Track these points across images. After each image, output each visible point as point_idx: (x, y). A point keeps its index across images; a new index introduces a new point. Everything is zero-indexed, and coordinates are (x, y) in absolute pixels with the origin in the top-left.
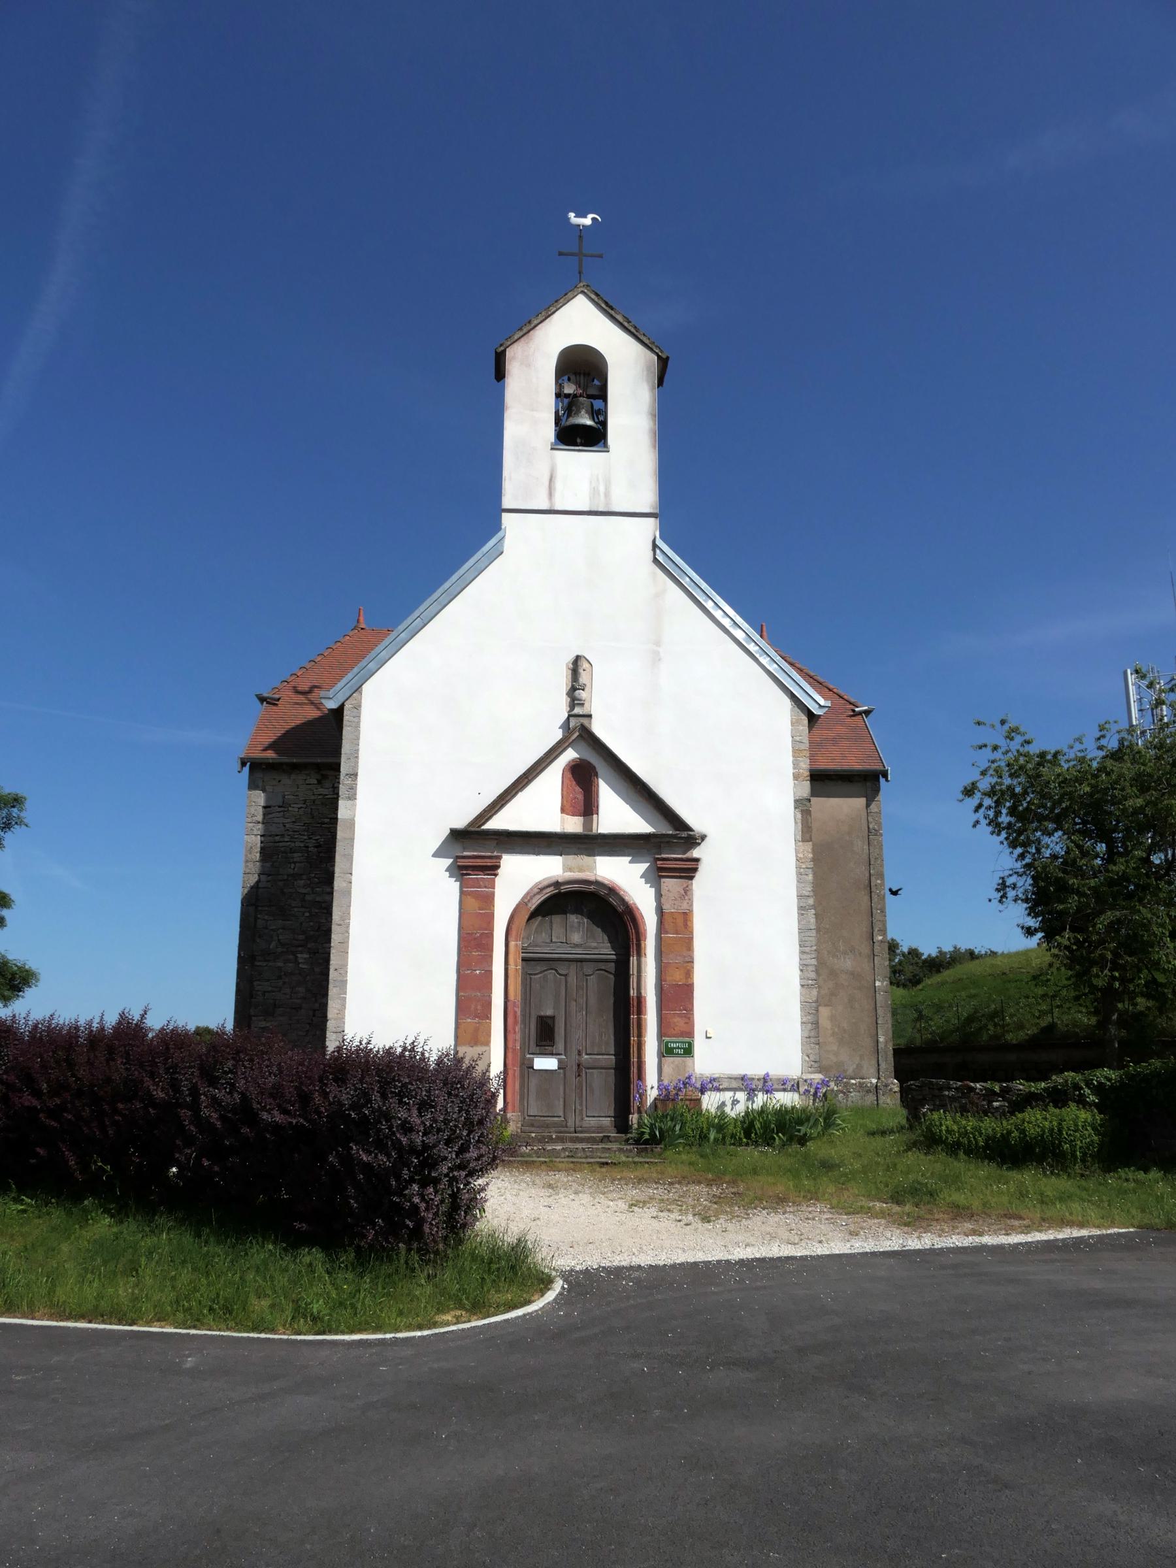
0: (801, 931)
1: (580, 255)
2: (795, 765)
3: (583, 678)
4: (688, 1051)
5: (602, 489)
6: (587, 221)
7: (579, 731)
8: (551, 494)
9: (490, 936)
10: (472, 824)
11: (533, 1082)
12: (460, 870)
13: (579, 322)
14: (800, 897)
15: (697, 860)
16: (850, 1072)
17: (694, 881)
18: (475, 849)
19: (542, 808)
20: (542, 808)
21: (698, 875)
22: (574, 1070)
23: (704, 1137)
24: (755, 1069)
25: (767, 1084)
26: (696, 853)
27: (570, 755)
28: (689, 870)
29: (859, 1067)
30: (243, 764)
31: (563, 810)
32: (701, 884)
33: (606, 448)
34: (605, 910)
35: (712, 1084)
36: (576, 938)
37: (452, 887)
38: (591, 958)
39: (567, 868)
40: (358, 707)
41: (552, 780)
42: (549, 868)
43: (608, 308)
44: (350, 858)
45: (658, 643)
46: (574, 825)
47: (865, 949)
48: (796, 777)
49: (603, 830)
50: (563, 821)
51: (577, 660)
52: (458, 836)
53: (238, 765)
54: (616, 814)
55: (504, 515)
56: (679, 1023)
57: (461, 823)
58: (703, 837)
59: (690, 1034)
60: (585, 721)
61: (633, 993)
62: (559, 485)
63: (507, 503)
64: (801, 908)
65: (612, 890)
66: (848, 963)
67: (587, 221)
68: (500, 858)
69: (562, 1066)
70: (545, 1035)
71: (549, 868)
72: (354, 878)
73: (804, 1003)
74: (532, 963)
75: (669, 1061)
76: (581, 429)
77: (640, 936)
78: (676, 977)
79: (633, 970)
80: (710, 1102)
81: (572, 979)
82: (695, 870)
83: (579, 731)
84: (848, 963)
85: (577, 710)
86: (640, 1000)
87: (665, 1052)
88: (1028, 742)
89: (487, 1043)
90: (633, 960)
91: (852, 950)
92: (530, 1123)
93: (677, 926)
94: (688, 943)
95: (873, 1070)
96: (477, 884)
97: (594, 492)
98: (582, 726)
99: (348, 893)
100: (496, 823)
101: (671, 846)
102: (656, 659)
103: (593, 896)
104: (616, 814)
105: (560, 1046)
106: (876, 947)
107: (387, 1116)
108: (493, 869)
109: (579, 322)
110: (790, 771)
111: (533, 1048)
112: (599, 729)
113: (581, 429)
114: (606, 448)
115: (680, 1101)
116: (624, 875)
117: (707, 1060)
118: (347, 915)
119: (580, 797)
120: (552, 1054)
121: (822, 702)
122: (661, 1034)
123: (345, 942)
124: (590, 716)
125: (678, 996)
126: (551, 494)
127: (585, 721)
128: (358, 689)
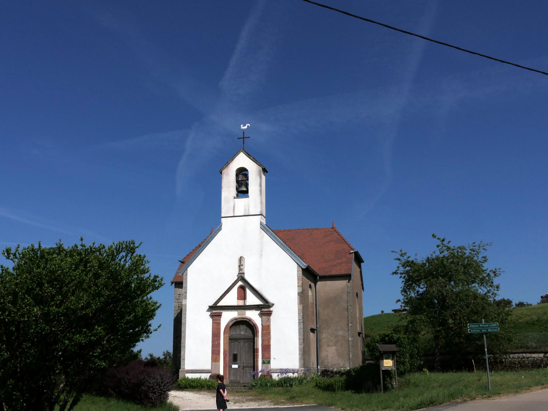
0: (299, 329)
1: (244, 138)
2: (298, 283)
3: (242, 263)
4: (269, 362)
5: (247, 209)
6: (246, 127)
7: (241, 277)
8: (234, 212)
9: (219, 333)
10: (214, 304)
11: (232, 371)
12: (212, 316)
13: (242, 160)
14: (299, 320)
15: (272, 311)
16: (341, 366)
17: (271, 317)
18: (216, 310)
19: (232, 299)
20: (232, 299)
21: (272, 315)
22: (243, 367)
23: (267, 385)
24: (285, 367)
25: (287, 371)
26: (271, 309)
27: (240, 283)
28: (269, 314)
29: (344, 364)
30: (172, 283)
31: (238, 299)
32: (272, 317)
33: (248, 197)
34: (249, 324)
35: (275, 371)
36: (242, 333)
37: (210, 321)
38: (243, 339)
39: (239, 315)
40: (187, 274)
41: (234, 292)
42: (234, 315)
43: (249, 155)
44: (185, 314)
45: (262, 251)
46: (241, 303)
47: (346, 329)
48: (298, 286)
49: (247, 304)
50: (238, 302)
51: (241, 257)
52: (211, 308)
53: (170, 283)
54: (252, 299)
55: (222, 219)
56: (267, 355)
57: (211, 304)
58: (273, 305)
59: (269, 358)
60: (242, 275)
61: (256, 347)
62: (236, 209)
63: (223, 215)
64: (299, 323)
65: (250, 320)
66: (341, 333)
67: (246, 127)
68: (221, 313)
69: (239, 367)
70: (235, 359)
71: (234, 315)
72: (187, 320)
73: (300, 349)
74: (232, 340)
75: (264, 365)
76: (242, 190)
77: (257, 332)
78: (266, 343)
79: (256, 341)
80: (275, 376)
81: (242, 344)
82: (271, 314)
83: (241, 277)
84: (341, 333)
85: (241, 272)
86: (257, 349)
87: (263, 363)
88: (409, 257)
89: (219, 361)
90: (256, 338)
91: (342, 329)
92: (231, 382)
93: (267, 329)
94: (269, 333)
95: (348, 365)
96: (216, 320)
97: (245, 209)
98: (242, 277)
99: (185, 324)
100: (220, 304)
101: (265, 308)
102: (261, 255)
103: (246, 321)
104: (252, 299)
105: (239, 362)
106: (350, 328)
107: (147, 381)
108: (220, 315)
109: (242, 160)
110: (297, 285)
111: (232, 362)
112: (247, 277)
113: (242, 190)
114: (248, 197)
115: (268, 374)
116: (254, 316)
117: (274, 364)
118: (185, 329)
119: (243, 295)
120: (236, 364)
121: (305, 264)
122: (262, 358)
123: (185, 336)
124: (244, 273)
125: (267, 348)
126: (234, 212)
127: (242, 275)
128: (186, 270)
